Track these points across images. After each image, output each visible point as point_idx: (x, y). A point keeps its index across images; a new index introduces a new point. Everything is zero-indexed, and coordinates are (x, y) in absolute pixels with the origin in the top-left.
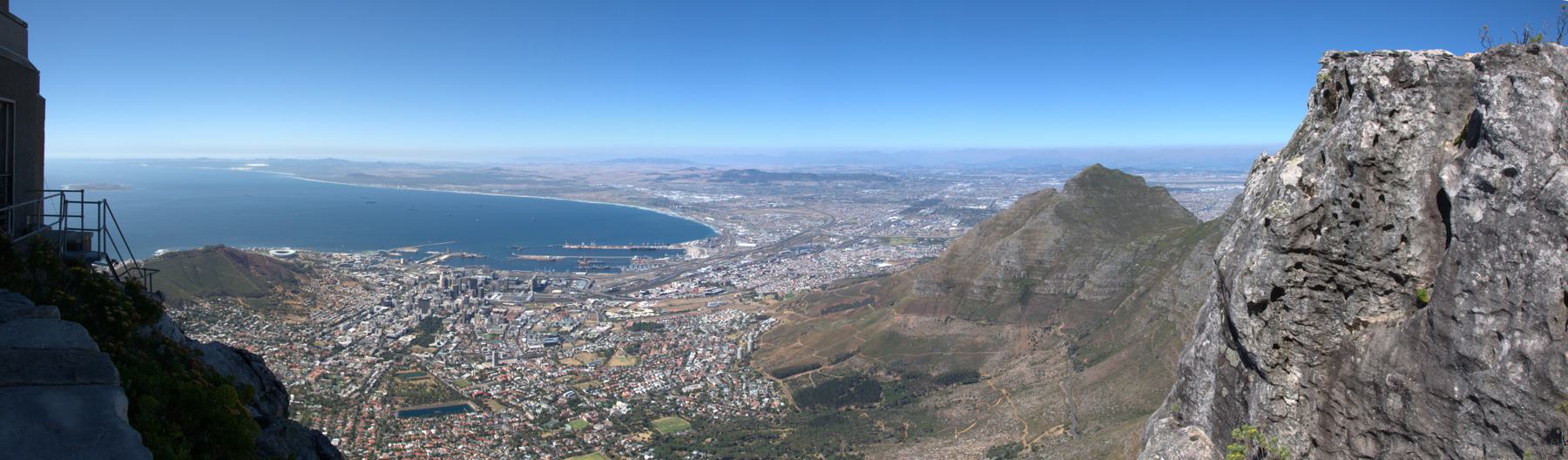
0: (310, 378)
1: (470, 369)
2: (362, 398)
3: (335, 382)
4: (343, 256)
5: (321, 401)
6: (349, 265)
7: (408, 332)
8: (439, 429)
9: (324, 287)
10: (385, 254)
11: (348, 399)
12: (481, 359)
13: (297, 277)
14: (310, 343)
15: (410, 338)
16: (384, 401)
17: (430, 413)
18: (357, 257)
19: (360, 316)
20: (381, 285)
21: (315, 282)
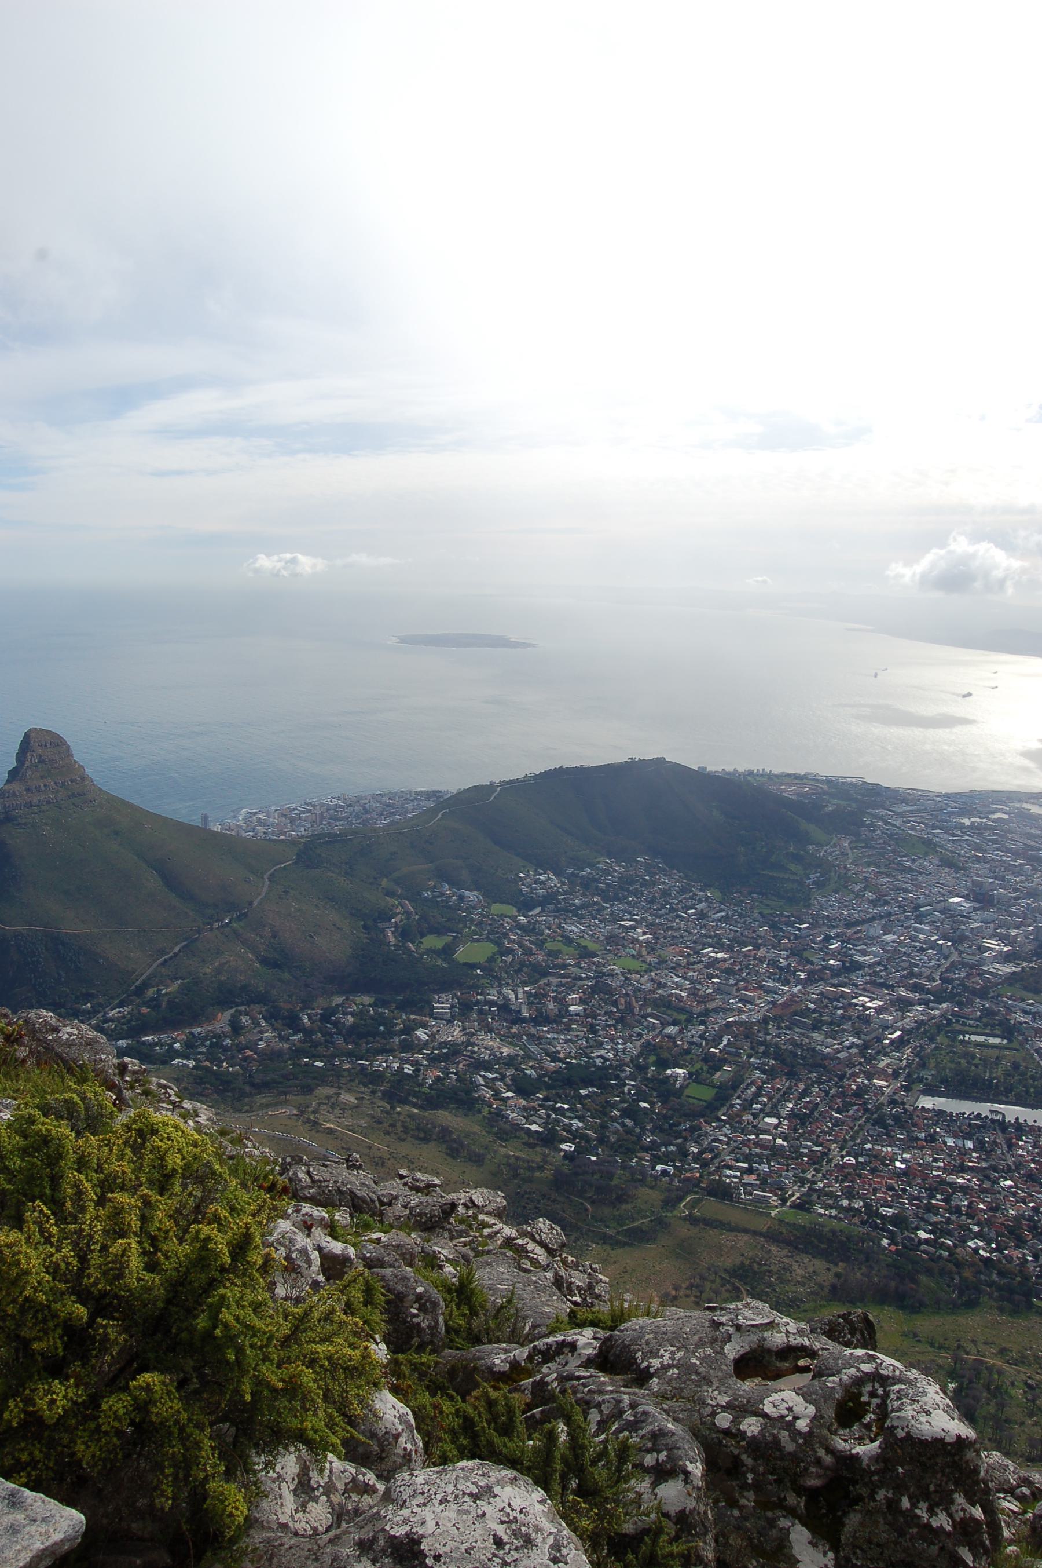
15: (1008, 969)
16: (896, 1075)
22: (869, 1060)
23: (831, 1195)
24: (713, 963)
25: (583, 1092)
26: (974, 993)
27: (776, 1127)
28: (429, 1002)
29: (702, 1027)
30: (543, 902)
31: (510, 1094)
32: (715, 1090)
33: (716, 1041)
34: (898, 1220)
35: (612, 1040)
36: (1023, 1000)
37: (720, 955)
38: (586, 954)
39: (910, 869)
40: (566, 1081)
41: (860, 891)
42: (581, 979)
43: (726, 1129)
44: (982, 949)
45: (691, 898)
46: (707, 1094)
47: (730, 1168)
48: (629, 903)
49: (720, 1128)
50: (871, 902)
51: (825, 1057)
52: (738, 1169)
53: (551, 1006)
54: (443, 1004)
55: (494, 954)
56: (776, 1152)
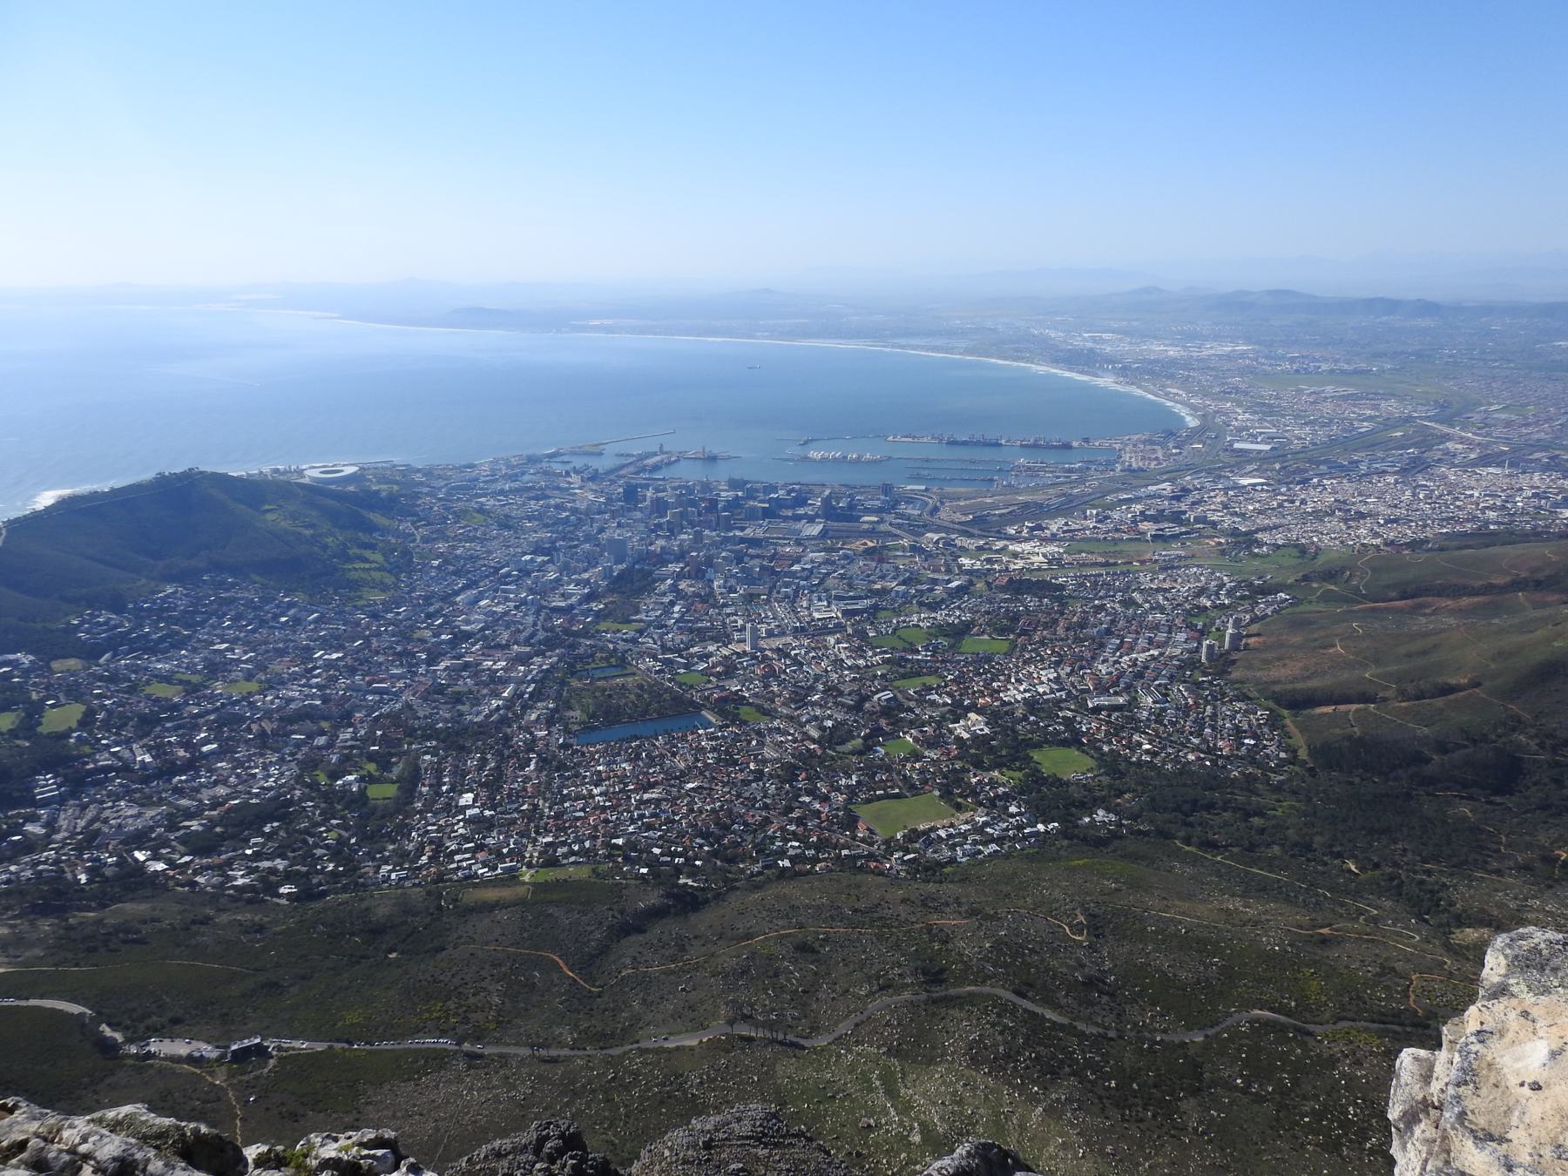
16: (550, 722)
22: (519, 717)
24: (330, 665)
25: (267, 829)
26: (576, 634)
27: (475, 800)
28: (30, 789)
30: (115, 644)
31: (187, 859)
34: (631, 845)
35: (265, 768)
37: (335, 656)
38: (192, 690)
40: (242, 823)
41: (439, 567)
44: (565, 596)
46: (390, 790)
47: (457, 852)
48: (212, 626)
51: (480, 725)
52: (467, 851)
53: (181, 753)
54: (47, 785)
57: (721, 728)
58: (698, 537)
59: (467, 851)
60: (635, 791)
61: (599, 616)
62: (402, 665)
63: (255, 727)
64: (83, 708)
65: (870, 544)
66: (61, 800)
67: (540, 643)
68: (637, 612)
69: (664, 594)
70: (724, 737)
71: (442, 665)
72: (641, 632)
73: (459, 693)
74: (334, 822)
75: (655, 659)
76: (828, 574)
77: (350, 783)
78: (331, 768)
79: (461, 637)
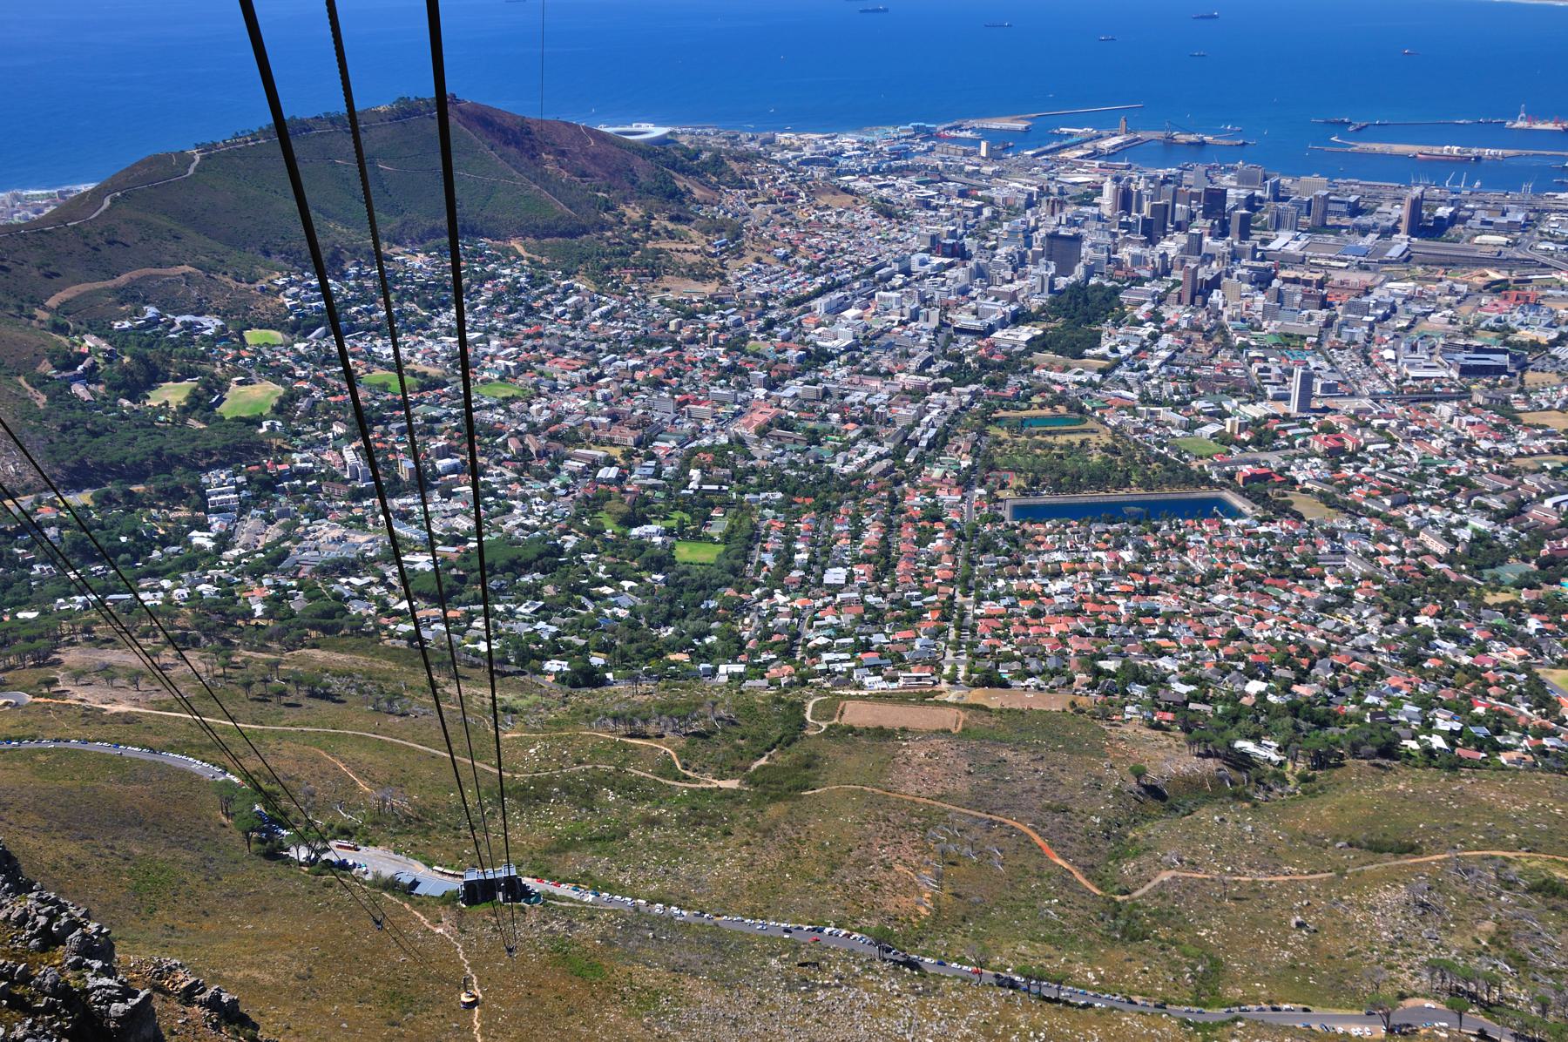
0: (738, 428)
1: (1222, 415)
2: (898, 474)
3: (814, 438)
4: (811, 142)
5: (780, 483)
6: (829, 160)
7: (1018, 319)
8: (1145, 553)
9: (760, 212)
10: (930, 135)
11: (859, 475)
12: (1257, 395)
13: (681, 182)
14: (736, 345)
15: (1025, 333)
16: (965, 482)
17: (1112, 512)
18: (848, 141)
19: (874, 278)
20: (926, 204)
21: (733, 199)
22: (912, 474)
23: (1009, 658)
25: (527, 579)
26: (1000, 367)
27: (850, 578)
29: (652, 463)
32: (721, 548)
33: (681, 477)
35: (525, 498)
36: (1066, 369)
39: (839, 226)
42: (438, 420)
43: (779, 598)
45: (553, 291)
47: (827, 648)
49: (770, 595)
50: (808, 269)
55: (282, 400)
56: (876, 618)
57: (1261, 521)
58: (1195, 246)
59: (842, 648)
60: (1127, 595)
61: (1035, 344)
62: (728, 385)
63: (513, 445)
64: (281, 390)
65: (1494, 275)
66: (244, 508)
67: (942, 374)
68: (1096, 343)
69: (1140, 324)
70: (1271, 536)
71: (789, 392)
72: (1104, 372)
73: (814, 432)
74: (627, 584)
75: (1134, 412)
76: (1426, 315)
77: (650, 535)
78: (624, 509)
79: (817, 357)
